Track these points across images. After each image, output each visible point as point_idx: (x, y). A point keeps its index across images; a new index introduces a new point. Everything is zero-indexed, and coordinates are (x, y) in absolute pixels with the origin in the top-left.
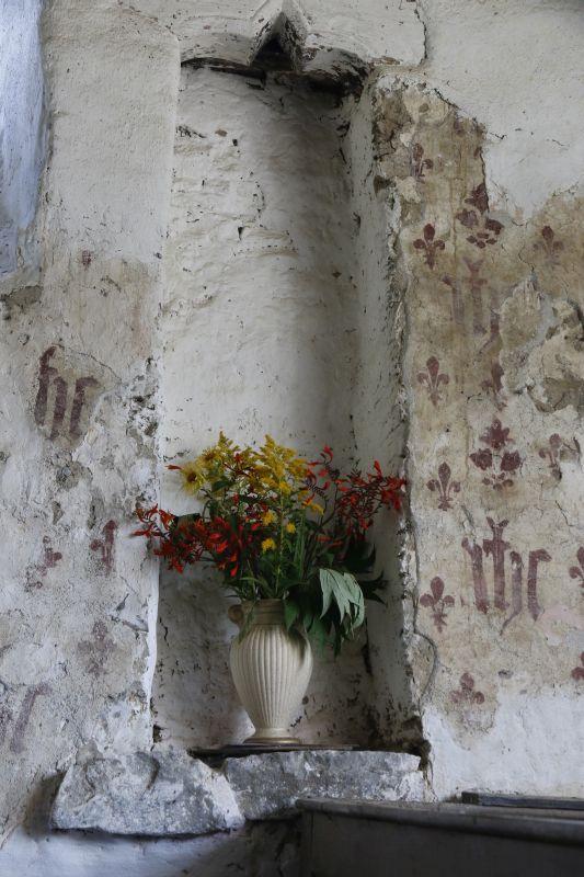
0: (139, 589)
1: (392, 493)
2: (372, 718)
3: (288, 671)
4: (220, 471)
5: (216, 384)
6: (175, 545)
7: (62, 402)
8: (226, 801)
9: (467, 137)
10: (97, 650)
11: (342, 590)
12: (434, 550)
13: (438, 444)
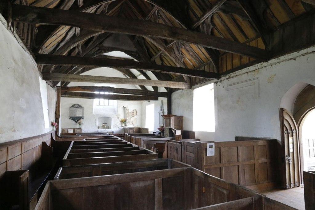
0: (120, 122)
1: (126, 120)
2: (126, 126)
3: (124, 124)
4: (122, 119)
5: (122, 117)
6: (121, 121)
7: (118, 118)
8: (122, 127)
9: (129, 110)
10: (119, 124)
11: (125, 122)
12: (127, 121)
13: (127, 119)
